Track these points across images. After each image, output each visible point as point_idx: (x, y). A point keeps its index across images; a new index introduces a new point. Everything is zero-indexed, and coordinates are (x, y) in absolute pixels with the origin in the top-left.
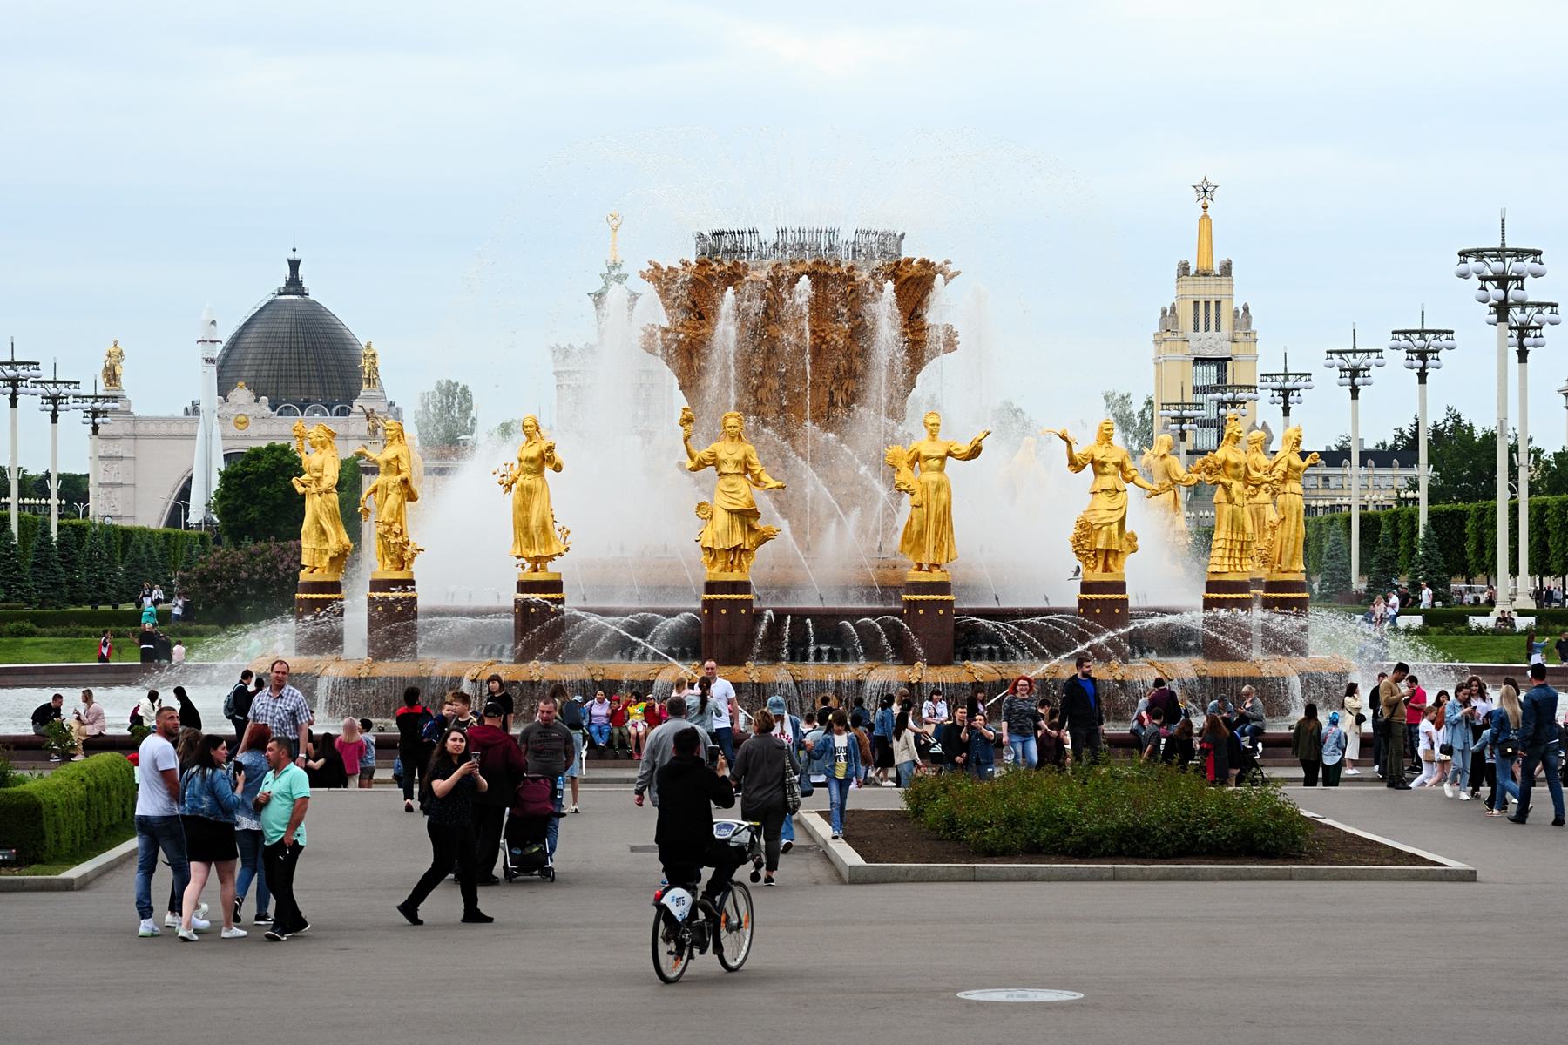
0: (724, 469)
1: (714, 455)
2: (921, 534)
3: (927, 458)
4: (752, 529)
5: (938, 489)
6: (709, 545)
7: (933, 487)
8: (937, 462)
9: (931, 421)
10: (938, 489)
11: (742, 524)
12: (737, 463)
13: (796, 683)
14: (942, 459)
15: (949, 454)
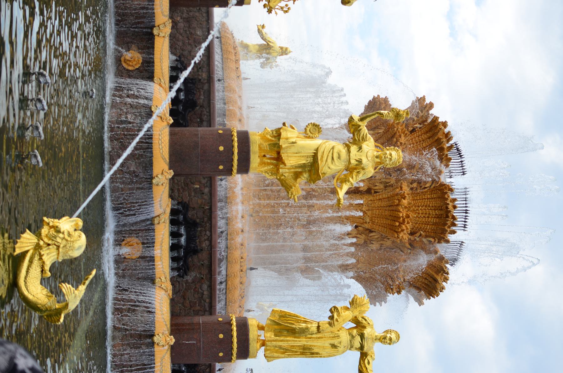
0: (354, 149)
1: (364, 139)
2: (293, 332)
3: (362, 336)
4: (297, 175)
5: (334, 346)
6: (284, 134)
7: (336, 342)
8: (357, 344)
9: (393, 336)
10: (334, 346)
11: (303, 166)
12: (360, 162)
13: (153, 219)
14: (362, 348)
15: (364, 355)
